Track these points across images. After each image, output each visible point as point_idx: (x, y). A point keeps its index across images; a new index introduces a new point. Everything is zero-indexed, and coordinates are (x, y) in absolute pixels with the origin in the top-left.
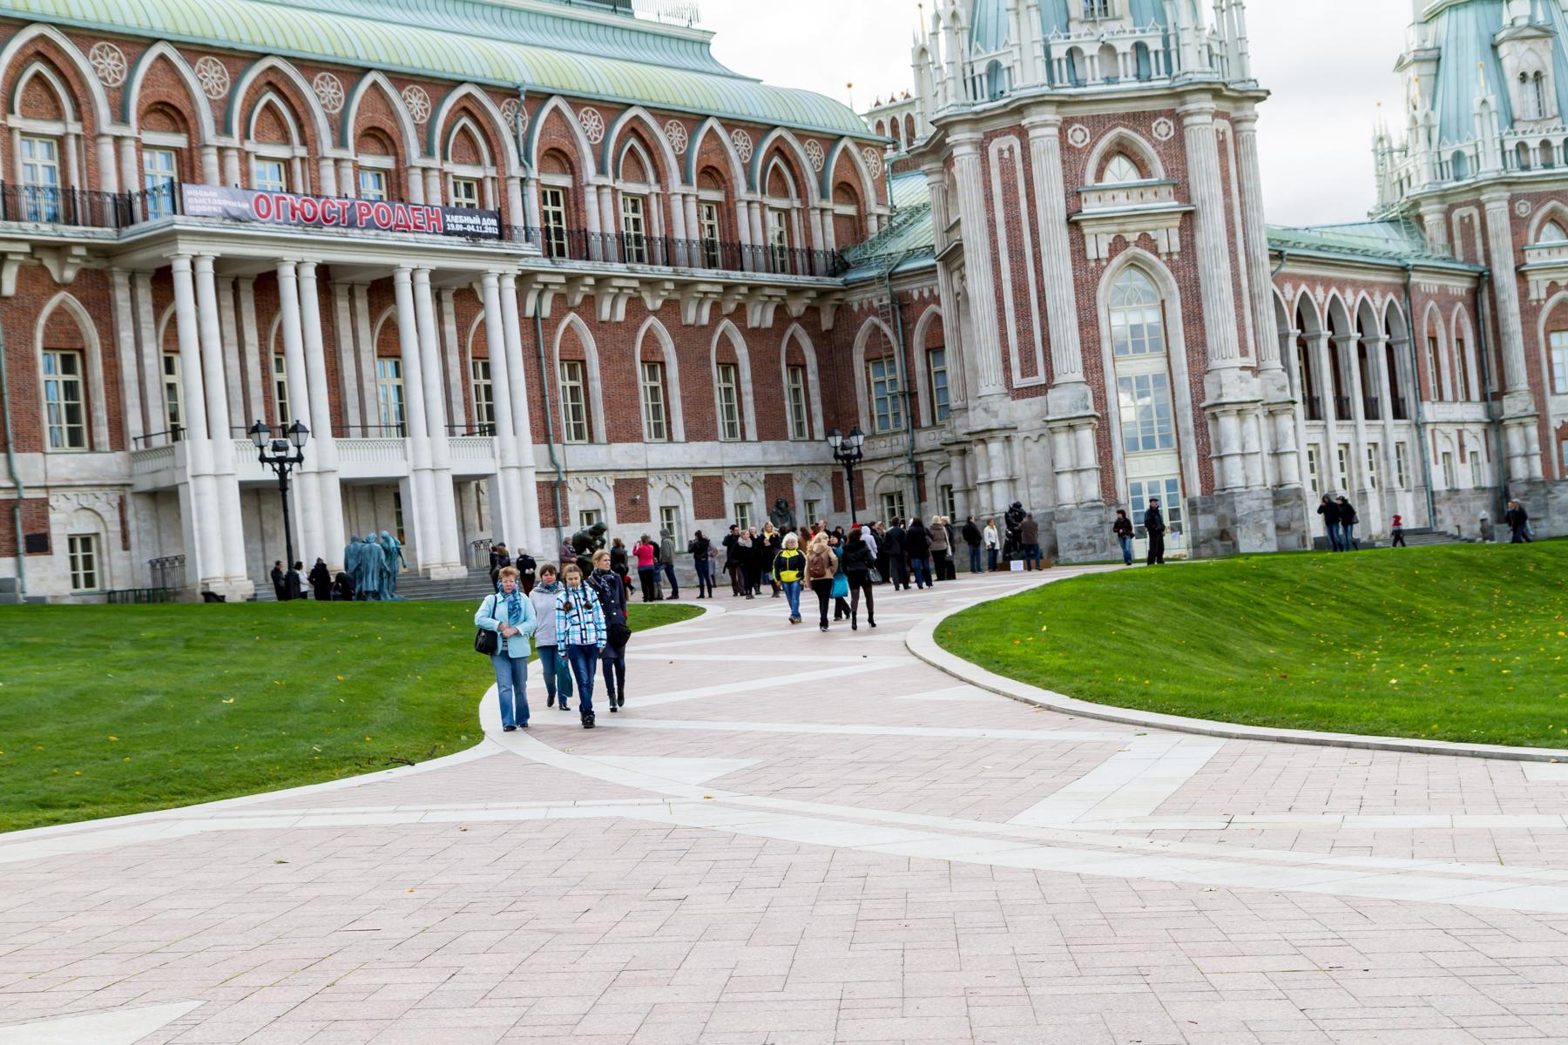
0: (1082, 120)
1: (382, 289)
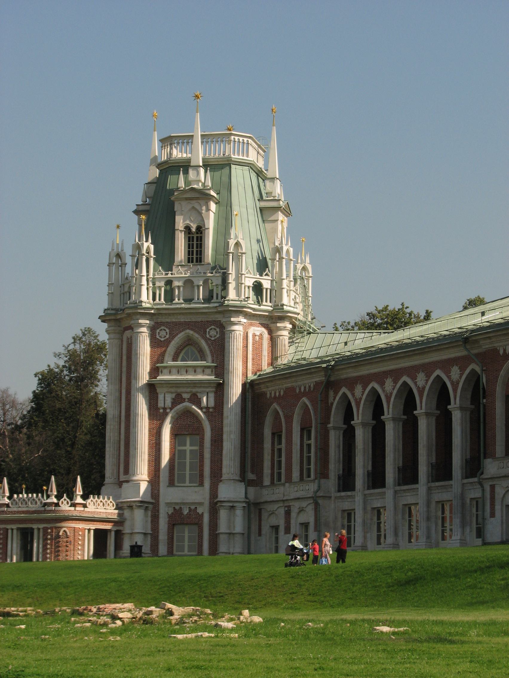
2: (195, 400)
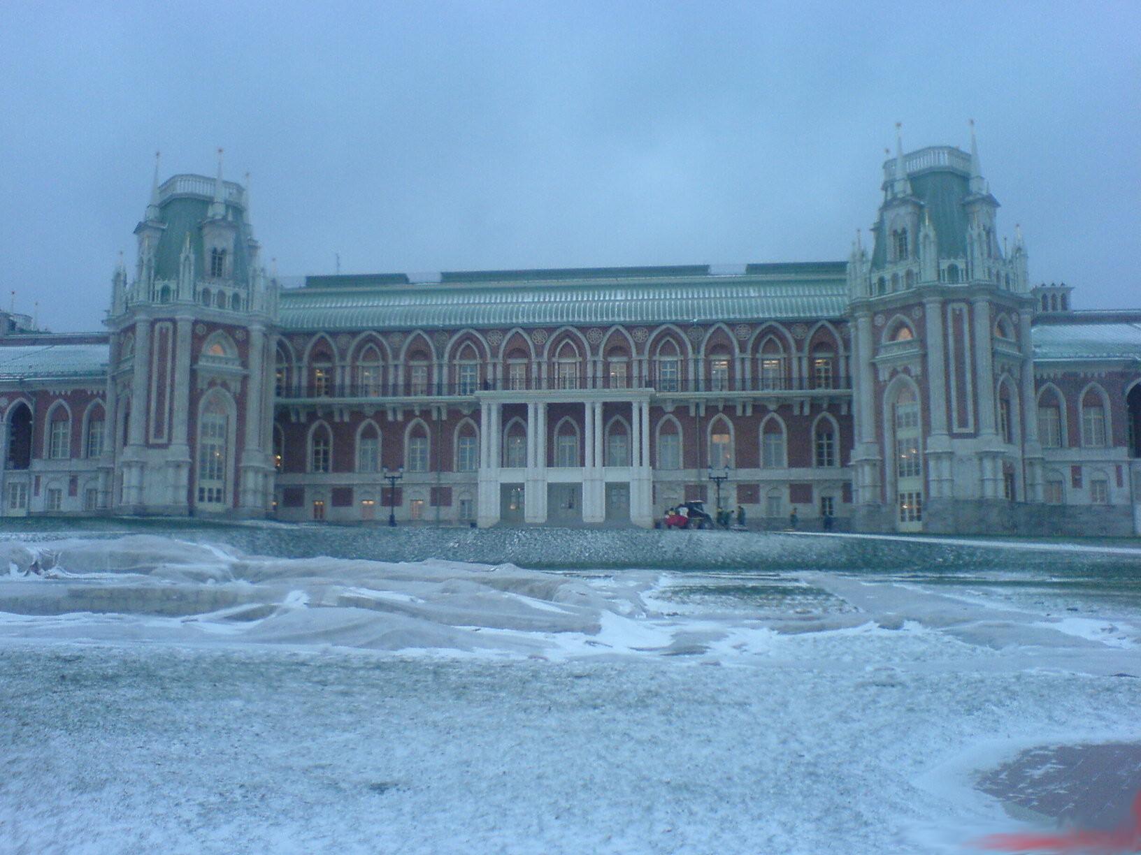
0: (881, 312)
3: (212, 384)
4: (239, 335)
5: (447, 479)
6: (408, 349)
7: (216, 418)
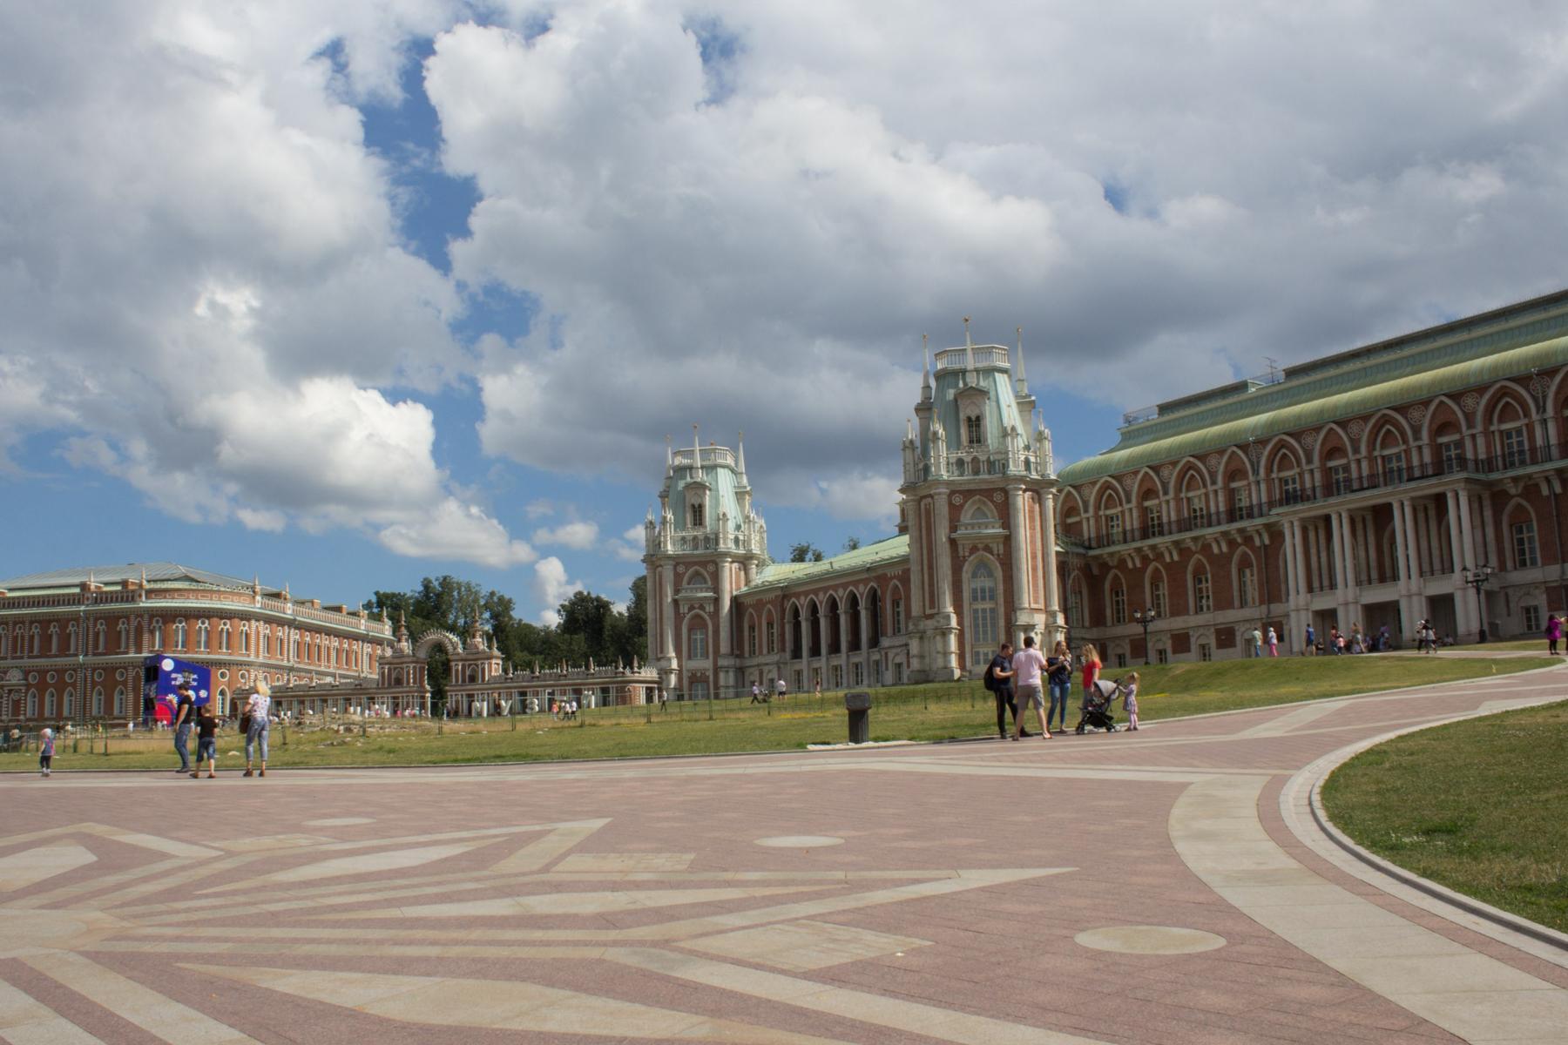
1: (1382, 514)
2: (702, 607)
3: (974, 549)
4: (998, 497)
5: (1277, 609)
6: (1225, 473)
7: (984, 583)
